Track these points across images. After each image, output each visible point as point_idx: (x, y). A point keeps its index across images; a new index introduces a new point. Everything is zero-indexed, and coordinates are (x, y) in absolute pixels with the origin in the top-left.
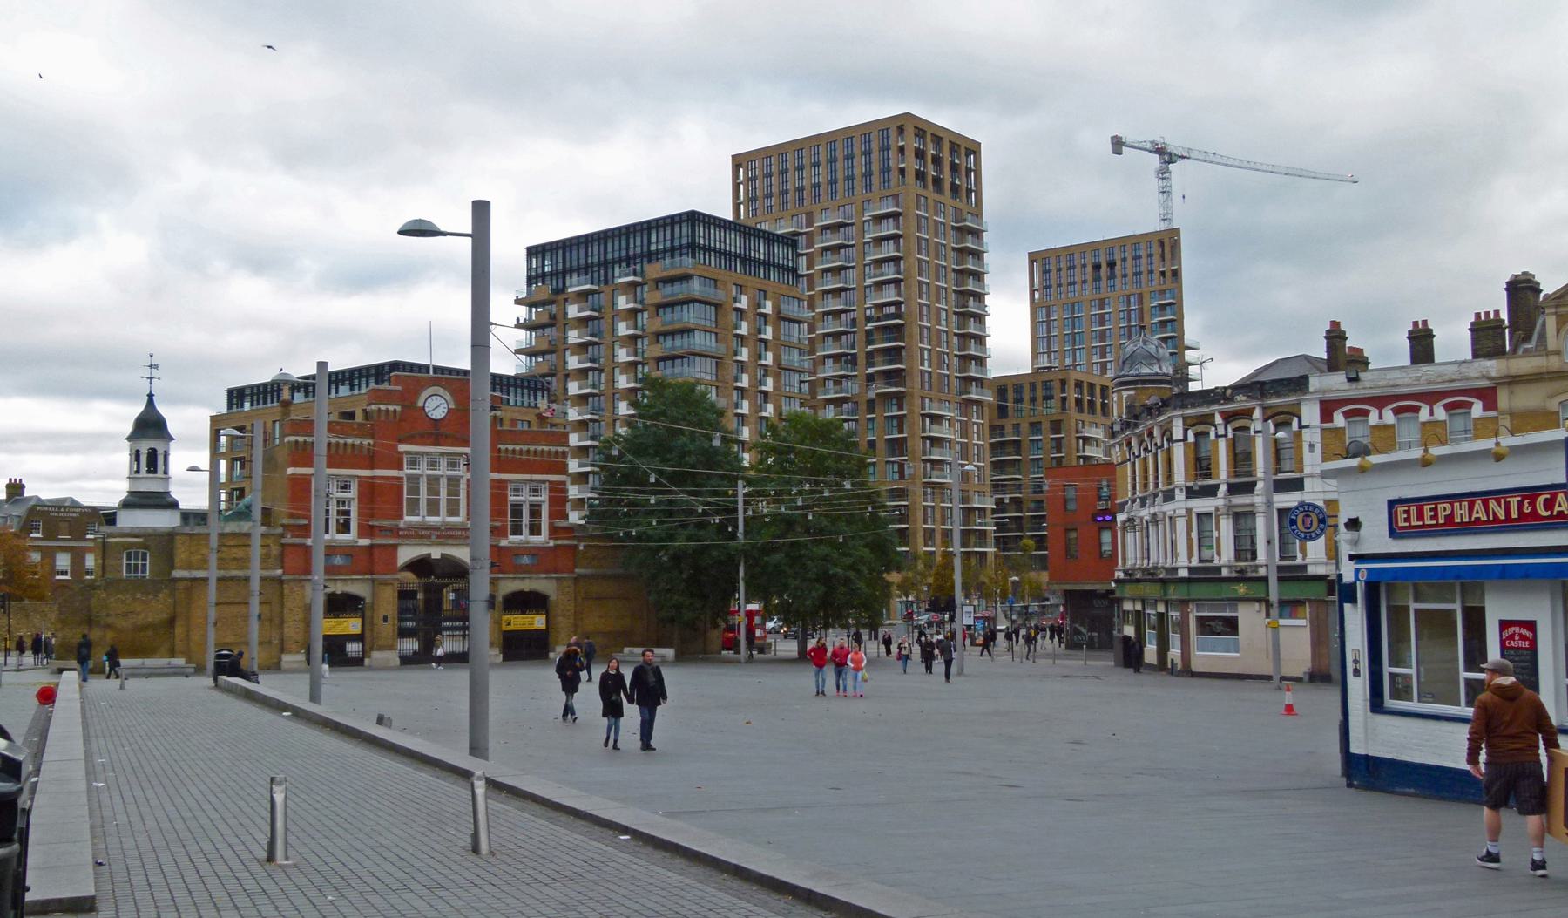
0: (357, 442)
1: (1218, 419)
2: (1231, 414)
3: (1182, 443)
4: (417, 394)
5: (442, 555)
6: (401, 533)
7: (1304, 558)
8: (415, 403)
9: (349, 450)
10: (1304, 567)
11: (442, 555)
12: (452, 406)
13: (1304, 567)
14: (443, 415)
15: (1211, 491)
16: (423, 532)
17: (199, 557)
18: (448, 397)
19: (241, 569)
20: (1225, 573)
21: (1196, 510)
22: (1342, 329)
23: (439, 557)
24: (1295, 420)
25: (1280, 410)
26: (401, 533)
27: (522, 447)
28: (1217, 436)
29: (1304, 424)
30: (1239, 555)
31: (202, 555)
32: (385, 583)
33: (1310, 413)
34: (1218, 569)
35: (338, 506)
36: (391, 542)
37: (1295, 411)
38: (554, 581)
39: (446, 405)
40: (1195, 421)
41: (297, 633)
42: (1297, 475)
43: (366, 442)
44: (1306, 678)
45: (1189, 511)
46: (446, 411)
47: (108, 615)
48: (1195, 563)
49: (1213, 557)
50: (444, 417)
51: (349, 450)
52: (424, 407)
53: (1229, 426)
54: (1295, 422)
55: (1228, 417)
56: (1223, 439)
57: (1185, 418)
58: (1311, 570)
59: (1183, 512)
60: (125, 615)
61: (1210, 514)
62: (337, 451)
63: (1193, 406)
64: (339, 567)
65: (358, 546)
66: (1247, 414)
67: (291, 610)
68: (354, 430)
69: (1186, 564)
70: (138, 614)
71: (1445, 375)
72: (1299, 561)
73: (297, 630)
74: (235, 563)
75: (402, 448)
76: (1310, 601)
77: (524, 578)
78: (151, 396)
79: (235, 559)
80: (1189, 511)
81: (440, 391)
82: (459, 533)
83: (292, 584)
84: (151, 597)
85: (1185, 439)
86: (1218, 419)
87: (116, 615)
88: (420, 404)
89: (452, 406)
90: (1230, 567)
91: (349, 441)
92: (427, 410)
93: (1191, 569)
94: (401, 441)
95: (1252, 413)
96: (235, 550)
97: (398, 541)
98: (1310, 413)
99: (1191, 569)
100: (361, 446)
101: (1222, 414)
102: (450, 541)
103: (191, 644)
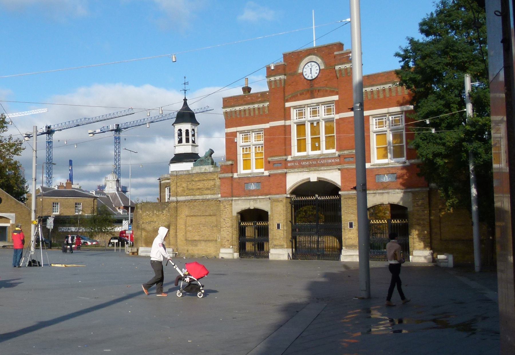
0: (261, 105)
4: (298, 63)
5: (318, 178)
6: (289, 165)
8: (296, 71)
9: (257, 112)
11: (318, 178)
12: (322, 67)
14: (316, 75)
16: (304, 163)
17: (182, 188)
18: (319, 61)
19: (202, 195)
23: (315, 180)
26: (289, 165)
27: (379, 87)
31: (183, 187)
32: (277, 201)
35: (243, 151)
36: (280, 171)
38: (410, 194)
39: (318, 68)
41: (228, 235)
43: (266, 104)
46: (318, 72)
47: (143, 223)
50: (317, 77)
51: (257, 112)
52: (303, 73)
60: (150, 223)
62: (250, 114)
64: (253, 191)
65: (264, 176)
67: (224, 220)
68: (259, 98)
70: (155, 222)
73: (228, 233)
74: (198, 191)
75: (288, 105)
77: (383, 193)
78: (185, 100)
79: (199, 189)
81: (313, 58)
82: (330, 161)
83: (225, 203)
84: (160, 213)
87: (146, 222)
88: (300, 71)
89: (322, 67)
91: (256, 106)
92: (304, 74)
94: (287, 101)
96: (199, 184)
97: (285, 170)
100: (264, 107)
102: (322, 168)
103: (178, 240)
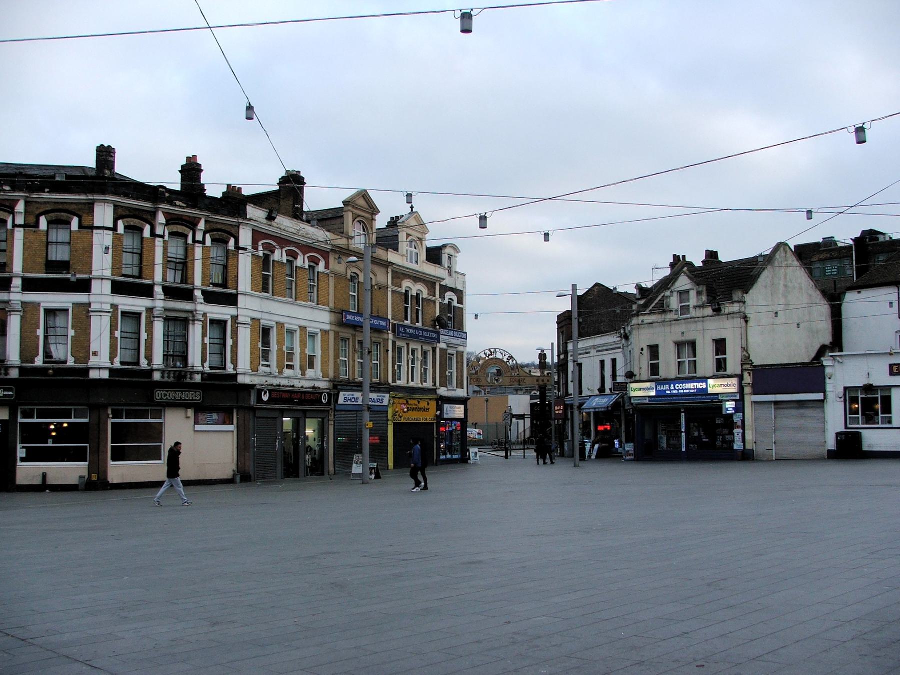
1: (161, 219)
2: (174, 217)
3: (111, 233)
7: (235, 369)
10: (235, 377)
13: (235, 377)
15: (147, 291)
20: (157, 376)
21: (122, 308)
22: (198, 163)
24: (232, 242)
25: (219, 227)
28: (153, 234)
29: (241, 245)
30: (290, 359)
33: (245, 237)
34: (149, 373)
37: (233, 231)
40: (128, 213)
42: (234, 292)
44: (238, 479)
45: (115, 307)
48: (117, 365)
49: (67, 359)
53: (166, 227)
54: (232, 242)
55: (171, 219)
56: (161, 240)
57: (116, 207)
58: (241, 380)
59: (108, 307)
61: (138, 316)
63: (127, 196)
66: (192, 224)
69: (109, 365)
71: (310, 235)
72: (230, 369)
76: (239, 409)
80: (115, 307)
85: (114, 229)
86: (161, 219)
90: (163, 372)
93: (112, 371)
95: (199, 222)
98: (245, 237)
99: (112, 371)
101: (166, 214)
